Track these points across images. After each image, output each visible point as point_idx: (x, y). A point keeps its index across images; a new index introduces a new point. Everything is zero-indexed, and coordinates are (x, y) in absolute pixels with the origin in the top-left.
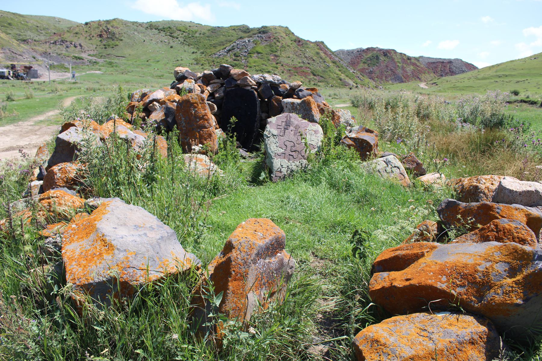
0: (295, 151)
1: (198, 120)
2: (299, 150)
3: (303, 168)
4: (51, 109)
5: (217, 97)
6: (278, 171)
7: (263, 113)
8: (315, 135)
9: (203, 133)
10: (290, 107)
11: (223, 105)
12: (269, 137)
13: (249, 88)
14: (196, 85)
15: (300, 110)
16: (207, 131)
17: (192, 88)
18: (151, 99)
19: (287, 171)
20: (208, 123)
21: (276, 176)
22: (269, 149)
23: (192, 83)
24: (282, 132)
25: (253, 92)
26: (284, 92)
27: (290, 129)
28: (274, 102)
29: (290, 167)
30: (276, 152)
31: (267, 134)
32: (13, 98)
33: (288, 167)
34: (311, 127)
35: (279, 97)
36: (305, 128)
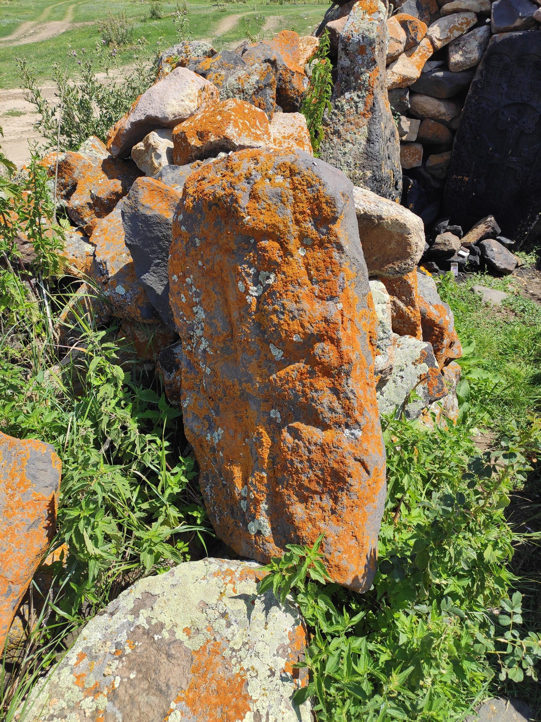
1: (277, 353)
4: (197, 37)
5: (456, 64)
9: (295, 450)
11: (470, 93)
14: (394, 21)
16: (323, 448)
17: (373, 35)
18: (137, 116)
20: (335, 391)
23: (376, 15)
32: (158, 12)
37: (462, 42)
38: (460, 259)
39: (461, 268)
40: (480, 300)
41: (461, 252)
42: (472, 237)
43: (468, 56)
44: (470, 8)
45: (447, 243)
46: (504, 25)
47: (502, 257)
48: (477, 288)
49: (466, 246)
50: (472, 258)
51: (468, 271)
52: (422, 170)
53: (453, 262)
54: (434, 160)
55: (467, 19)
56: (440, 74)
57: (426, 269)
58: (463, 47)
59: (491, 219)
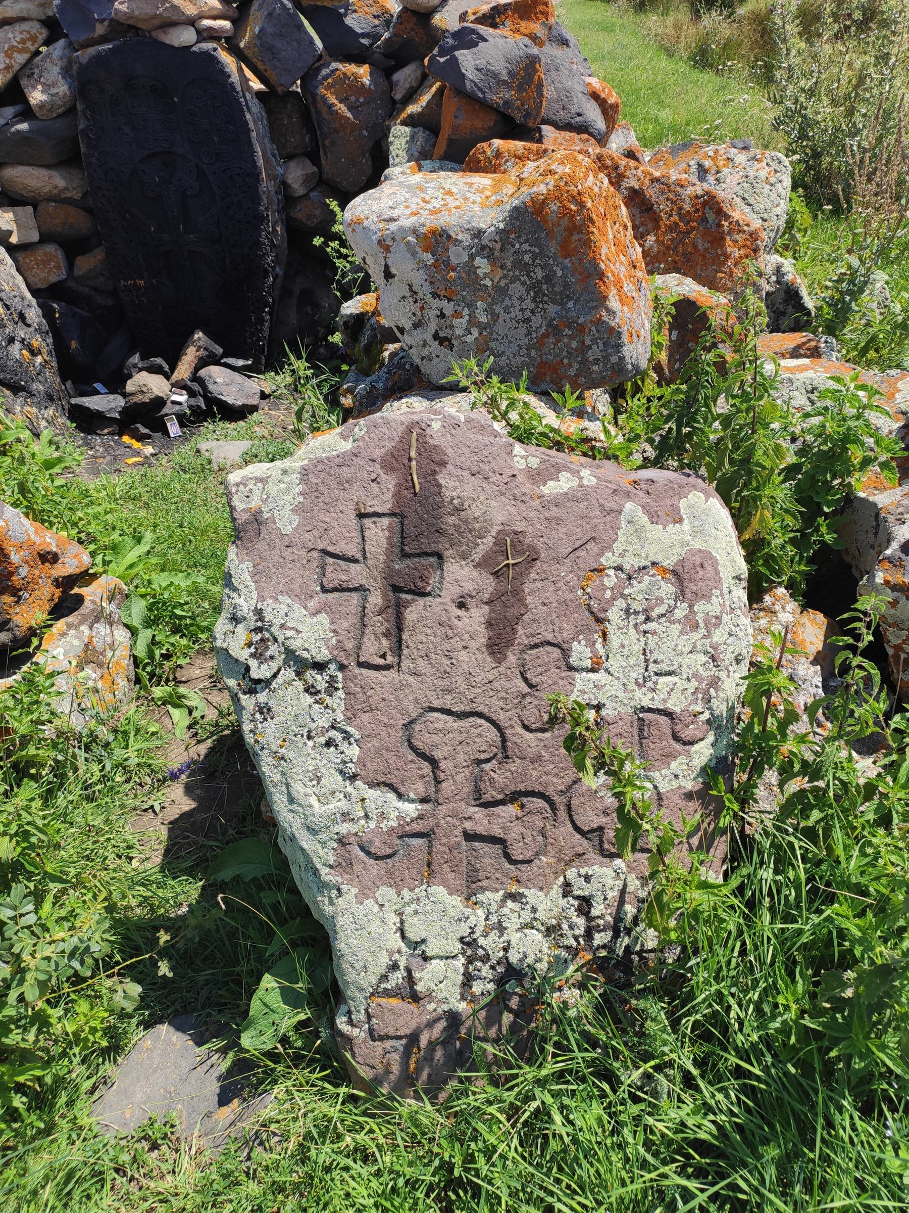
0: (514, 797)
3: (600, 939)
5: (42, 105)
6: (387, 993)
7: (292, 164)
8: (681, 611)
10: (418, 278)
11: (83, 150)
12: (266, 683)
13: (185, 37)
15: (502, 292)
19: (468, 979)
22: (279, 802)
24: (378, 624)
25: (210, 59)
26: (375, 37)
27: (450, 592)
28: (333, 100)
29: (490, 943)
30: (344, 828)
31: (244, 655)
33: (468, 942)
34: (639, 532)
35: (351, 68)
36: (586, 558)
37: (36, 71)
38: (177, 407)
39: (183, 420)
40: (210, 462)
41: (175, 398)
42: (183, 371)
43: (54, 91)
44: (25, 14)
45: (145, 389)
46: (84, 37)
48: (203, 446)
49: (181, 386)
50: (193, 402)
51: (194, 423)
52: (72, 284)
53: (167, 415)
54: (85, 264)
55: (28, 32)
56: (24, 126)
57: (132, 437)
58: (40, 77)
59: (198, 335)
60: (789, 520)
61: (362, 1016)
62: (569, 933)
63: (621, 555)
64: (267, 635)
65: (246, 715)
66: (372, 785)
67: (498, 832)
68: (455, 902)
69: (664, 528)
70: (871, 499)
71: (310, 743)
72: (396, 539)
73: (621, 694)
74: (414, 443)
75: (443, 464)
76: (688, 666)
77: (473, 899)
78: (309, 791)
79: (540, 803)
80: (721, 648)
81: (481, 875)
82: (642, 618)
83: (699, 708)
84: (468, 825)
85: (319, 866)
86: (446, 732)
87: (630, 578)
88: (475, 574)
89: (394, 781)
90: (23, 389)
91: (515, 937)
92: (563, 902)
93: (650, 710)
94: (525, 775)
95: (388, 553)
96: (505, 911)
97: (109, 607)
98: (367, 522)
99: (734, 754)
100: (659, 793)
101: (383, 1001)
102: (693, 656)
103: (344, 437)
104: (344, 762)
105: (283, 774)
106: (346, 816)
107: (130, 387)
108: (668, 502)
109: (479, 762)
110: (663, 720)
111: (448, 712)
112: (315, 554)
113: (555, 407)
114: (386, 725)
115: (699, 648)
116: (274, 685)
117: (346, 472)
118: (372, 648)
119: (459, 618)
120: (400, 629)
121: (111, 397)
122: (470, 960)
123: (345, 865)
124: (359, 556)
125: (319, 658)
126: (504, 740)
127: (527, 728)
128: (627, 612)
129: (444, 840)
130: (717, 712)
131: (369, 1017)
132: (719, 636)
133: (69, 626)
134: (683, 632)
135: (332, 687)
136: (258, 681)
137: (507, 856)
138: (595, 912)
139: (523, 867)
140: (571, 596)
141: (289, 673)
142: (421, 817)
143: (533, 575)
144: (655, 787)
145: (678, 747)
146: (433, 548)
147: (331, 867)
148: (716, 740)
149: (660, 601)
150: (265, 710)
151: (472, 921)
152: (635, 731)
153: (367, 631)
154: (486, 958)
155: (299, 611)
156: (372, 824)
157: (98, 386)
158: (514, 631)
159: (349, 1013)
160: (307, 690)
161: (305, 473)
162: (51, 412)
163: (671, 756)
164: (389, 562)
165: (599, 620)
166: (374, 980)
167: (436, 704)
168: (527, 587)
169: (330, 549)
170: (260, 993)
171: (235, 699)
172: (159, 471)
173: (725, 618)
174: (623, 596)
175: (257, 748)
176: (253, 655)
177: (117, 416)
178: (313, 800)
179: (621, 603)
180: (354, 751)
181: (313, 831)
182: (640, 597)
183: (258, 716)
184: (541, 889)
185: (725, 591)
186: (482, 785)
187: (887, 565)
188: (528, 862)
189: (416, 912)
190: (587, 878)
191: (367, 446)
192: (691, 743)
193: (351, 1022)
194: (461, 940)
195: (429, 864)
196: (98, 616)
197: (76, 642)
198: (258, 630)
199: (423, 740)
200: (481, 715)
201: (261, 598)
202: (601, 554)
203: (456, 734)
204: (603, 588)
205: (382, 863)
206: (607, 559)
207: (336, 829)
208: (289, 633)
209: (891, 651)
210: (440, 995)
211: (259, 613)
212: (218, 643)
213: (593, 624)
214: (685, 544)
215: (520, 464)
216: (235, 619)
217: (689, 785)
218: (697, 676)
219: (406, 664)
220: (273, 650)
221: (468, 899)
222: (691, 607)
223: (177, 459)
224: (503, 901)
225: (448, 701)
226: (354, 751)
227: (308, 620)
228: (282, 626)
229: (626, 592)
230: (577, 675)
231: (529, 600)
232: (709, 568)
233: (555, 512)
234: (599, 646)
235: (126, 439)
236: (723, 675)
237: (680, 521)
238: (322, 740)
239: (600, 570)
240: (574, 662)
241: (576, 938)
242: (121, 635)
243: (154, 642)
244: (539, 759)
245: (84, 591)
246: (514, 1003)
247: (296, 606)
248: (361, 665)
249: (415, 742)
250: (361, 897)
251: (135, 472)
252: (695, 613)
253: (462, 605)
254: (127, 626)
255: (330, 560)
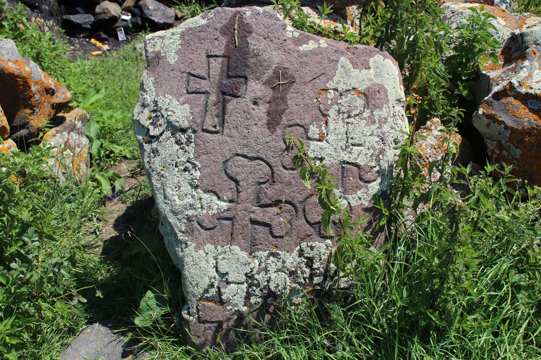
0: (277, 203)
2: (298, 198)
3: (316, 280)
6: (208, 299)
12: (156, 138)
19: (248, 296)
21: (200, 321)
24: (214, 110)
27: (249, 96)
29: (260, 277)
30: (190, 212)
31: (146, 123)
33: (249, 276)
34: (347, 72)
38: (125, 23)
41: (124, 17)
45: (106, 11)
47: (159, 13)
49: (127, 10)
50: (134, 20)
51: (134, 32)
53: (118, 27)
57: (97, 40)
60: (444, 83)
61: (195, 310)
62: (301, 276)
63: (337, 83)
64: (159, 114)
65: (146, 154)
66: (205, 192)
67: (267, 220)
68: (244, 255)
69: (360, 71)
70: (488, 74)
71: (176, 169)
72: (225, 68)
73: (333, 153)
74: (237, 22)
75: (250, 32)
76: (369, 142)
77: (253, 254)
78: (174, 193)
79: (289, 207)
80: (387, 134)
81: (258, 242)
82: (346, 115)
83: (373, 164)
84: (252, 216)
85: (177, 232)
86: (243, 166)
87: (341, 95)
88: (263, 88)
89: (217, 190)
90: (37, 8)
91: (273, 276)
92: (298, 259)
93: (348, 163)
94: (282, 192)
95: (221, 75)
96: (269, 261)
97: (79, 124)
98: (212, 60)
99: (391, 190)
100: (351, 207)
101: (205, 303)
102: (372, 137)
103: (203, 18)
104: (192, 179)
105: (162, 184)
106: (192, 206)
107: (98, 9)
108: (364, 58)
109: (260, 183)
110: (354, 168)
111: (245, 157)
112: (185, 75)
113: (320, 14)
114: (214, 162)
115: (375, 133)
116: (161, 139)
117: (203, 35)
118: (210, 122)
119: (253, 109)
120: (224, 113)
121: (86, 15)
122: (250, 286)
123: (190, 232)
124: (206, 76)
125: (183, 126)
126: (273, 173)
127: (284, 167)
128: (339, 111)
129: (240, 222)
130: (383, 167)
131: (198, 311)
132: (386, 128)
133: (57, 132)
134: (367, 124)
135: (189, 142)
136: (153, 137)
137: (272, 233)
138: (315, 266)
139: (279, 240)
140: (309, 102)
141: (168, 134)
142: (229, 210)
143: (292, 90)
144: (349, 203)
145: (362, 183)
146: (243, 73)
147: (183, 232)
148: (382, 182)
149: (356, 107)
150: (155, 152)
151: (252, 265)
152: (340, 173)
153: (208, 114)
154: (258, 285)
155: (175, 102)
156: (205, 212)
157: (79, 9)
158: (281, 118)
159: (189, 309)
160: (176, 142)
161: (183, 34)
162: (51, 22)
163: (358, 188)
164: (221, 79)
165: (324, 115)
166: (201, 291)
167: (240, 152)
168: (289, 96)
169: (192, 72)
170: (145, 298)
171: (141, 146)
172: (111, 60)
173: (390, 119)
174: (337, 104)
175: (150, 170)
176: (151, 124)
177: (89, 26)
178: (176, 198)
179: (336, 107)
180: (198, 174)
181: (175, 213)
182: (346, 105)
183: (152, 154)
184: (288, 252)
185: (391, 106)
186: (260, 196)
187: (485, 105)
188: (282, 237)
189: (224, 258)
190: (312, 248)
191: (214, 22)
192: (369, 182)
193: (189, 314)
194: (246, 275)
195: (232, 234)
196: (73, 128)
197: (61, 140)
198: (155, 111)
199: (233, 170)
200: (262, 159)
201: (157, 95)
202: (327, 82)
203: (249, 168)
204: (327, 99)
205: (208, 232)
206: (330, 85)
207: (187, 213)
208: (169, 113)
209: (490, 154)
210: (234, 302)
211: (156, 103)
212: (135, 118)
213: (321, 117)
214: (370, 80)
215: (290, 35)
216: (144, 106)
217: (366, 204)
218: (373, 147)
219: (226, 131)
220: (161, 121)
221: (251, 254)
222: (372, 112)
223: (122, 53)
224: (268, 256)
225: (245, 151)
226: (198, 174)
227: (179, 107)
228: (167, 110)
229: (339, 102)
230: (312, 142)
231: (289, 102)
232: (382, 93)
233: (305, 59)
234: (323, 128)
235: (93, 41)
236: (387, 148)
237: (369, 68)
238: (182, 168)
239: (326, 90)
240: (310, 134)
241: (305, 279)
242: (84, 141)
243: (101, 146)
244: (289, 184)
245: (66, 115)
246: (271, 309)
247: (174, 100)
248: (204, 131)
249: (228, 171)
250: (197, 248)
251: (97, 59)
252: (374, 115)
253: (255, 103)
254: (87, 137)
255: (192, 78)
